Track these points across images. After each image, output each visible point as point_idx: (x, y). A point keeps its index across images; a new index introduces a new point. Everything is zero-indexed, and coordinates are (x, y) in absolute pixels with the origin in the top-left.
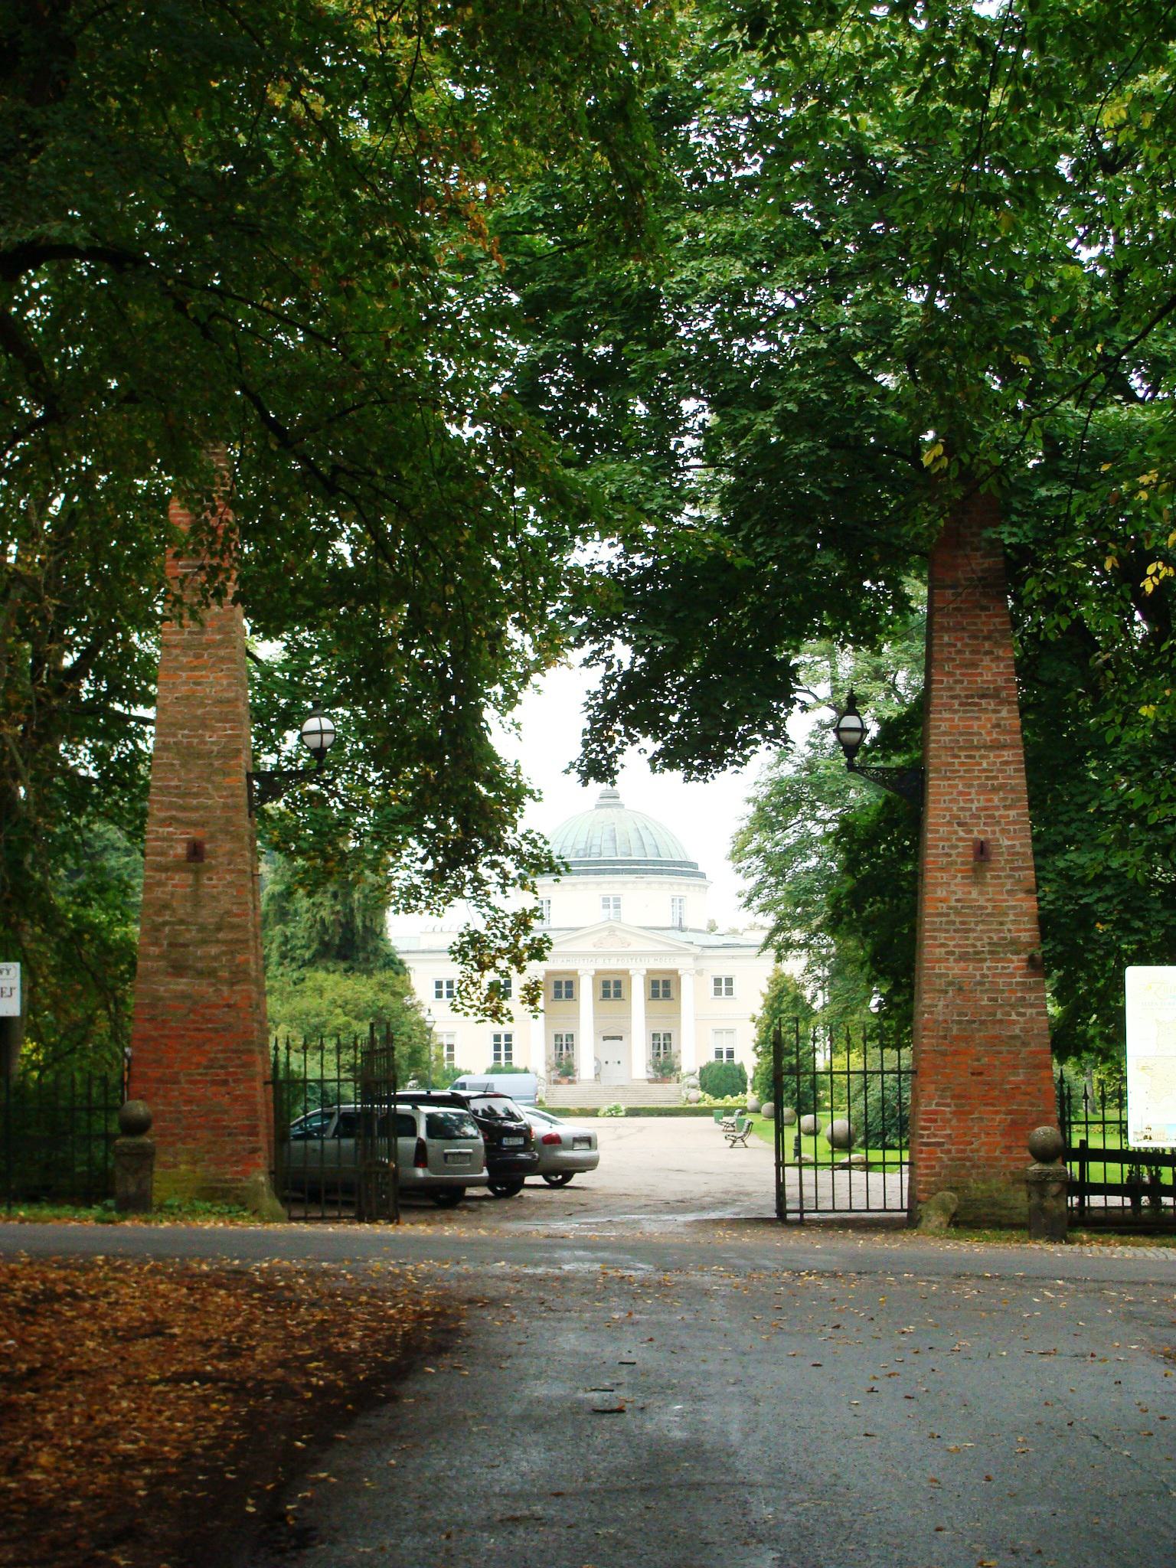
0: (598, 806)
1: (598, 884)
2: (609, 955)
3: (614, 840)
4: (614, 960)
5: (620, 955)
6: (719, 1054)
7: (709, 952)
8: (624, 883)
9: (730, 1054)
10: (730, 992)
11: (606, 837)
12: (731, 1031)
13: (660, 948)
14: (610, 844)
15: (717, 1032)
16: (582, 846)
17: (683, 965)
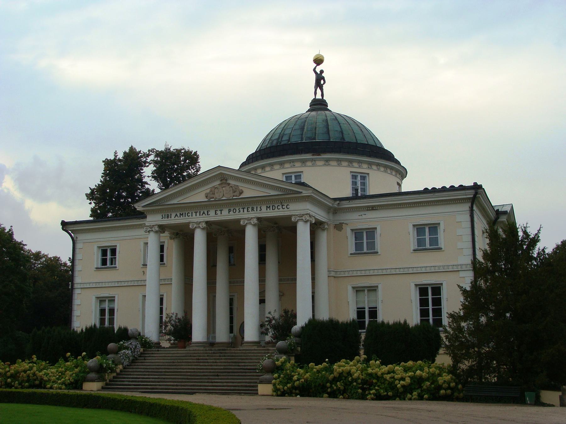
1: (282, 164)
2: (218, 205)
3: (302, 129)
4: (225, 212)
5: (231, 204)
6: (361, 313)
7: (346, 205)
8: (304, 162)
9: (373, 313)
10: (372, 245)
11: (297, 127)
12: (373, 289)
13: (273, 193)
14: (299, 132)
15: (358, 290)
16: (277, 137)
17: (295, 209)
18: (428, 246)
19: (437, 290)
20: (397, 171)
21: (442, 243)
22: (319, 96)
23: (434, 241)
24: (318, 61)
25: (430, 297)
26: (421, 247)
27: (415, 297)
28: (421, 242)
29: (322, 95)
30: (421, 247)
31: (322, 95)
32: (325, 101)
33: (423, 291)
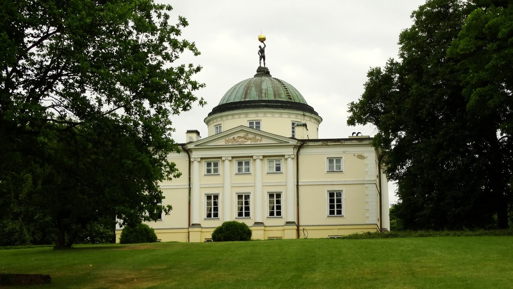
0: (256, 76)
18: (335, 170)
19: (339, 194)
20: (316, 119)
21: (343, 168)
22: (263, 66)
23: (339, 167)
24: (262, 40)
25: (335, 198)
26: (331, 171)
27: (327, 198)
28: (331, 167)
29: (264, 64)
30: (331, 171)
31: (264, 64)
32: (267, 69)
33: (331, 195)
